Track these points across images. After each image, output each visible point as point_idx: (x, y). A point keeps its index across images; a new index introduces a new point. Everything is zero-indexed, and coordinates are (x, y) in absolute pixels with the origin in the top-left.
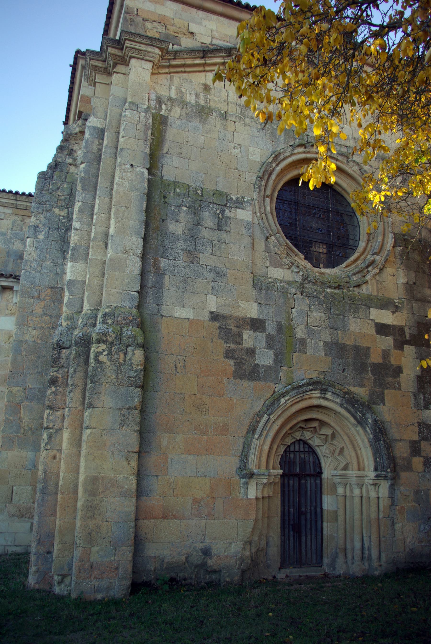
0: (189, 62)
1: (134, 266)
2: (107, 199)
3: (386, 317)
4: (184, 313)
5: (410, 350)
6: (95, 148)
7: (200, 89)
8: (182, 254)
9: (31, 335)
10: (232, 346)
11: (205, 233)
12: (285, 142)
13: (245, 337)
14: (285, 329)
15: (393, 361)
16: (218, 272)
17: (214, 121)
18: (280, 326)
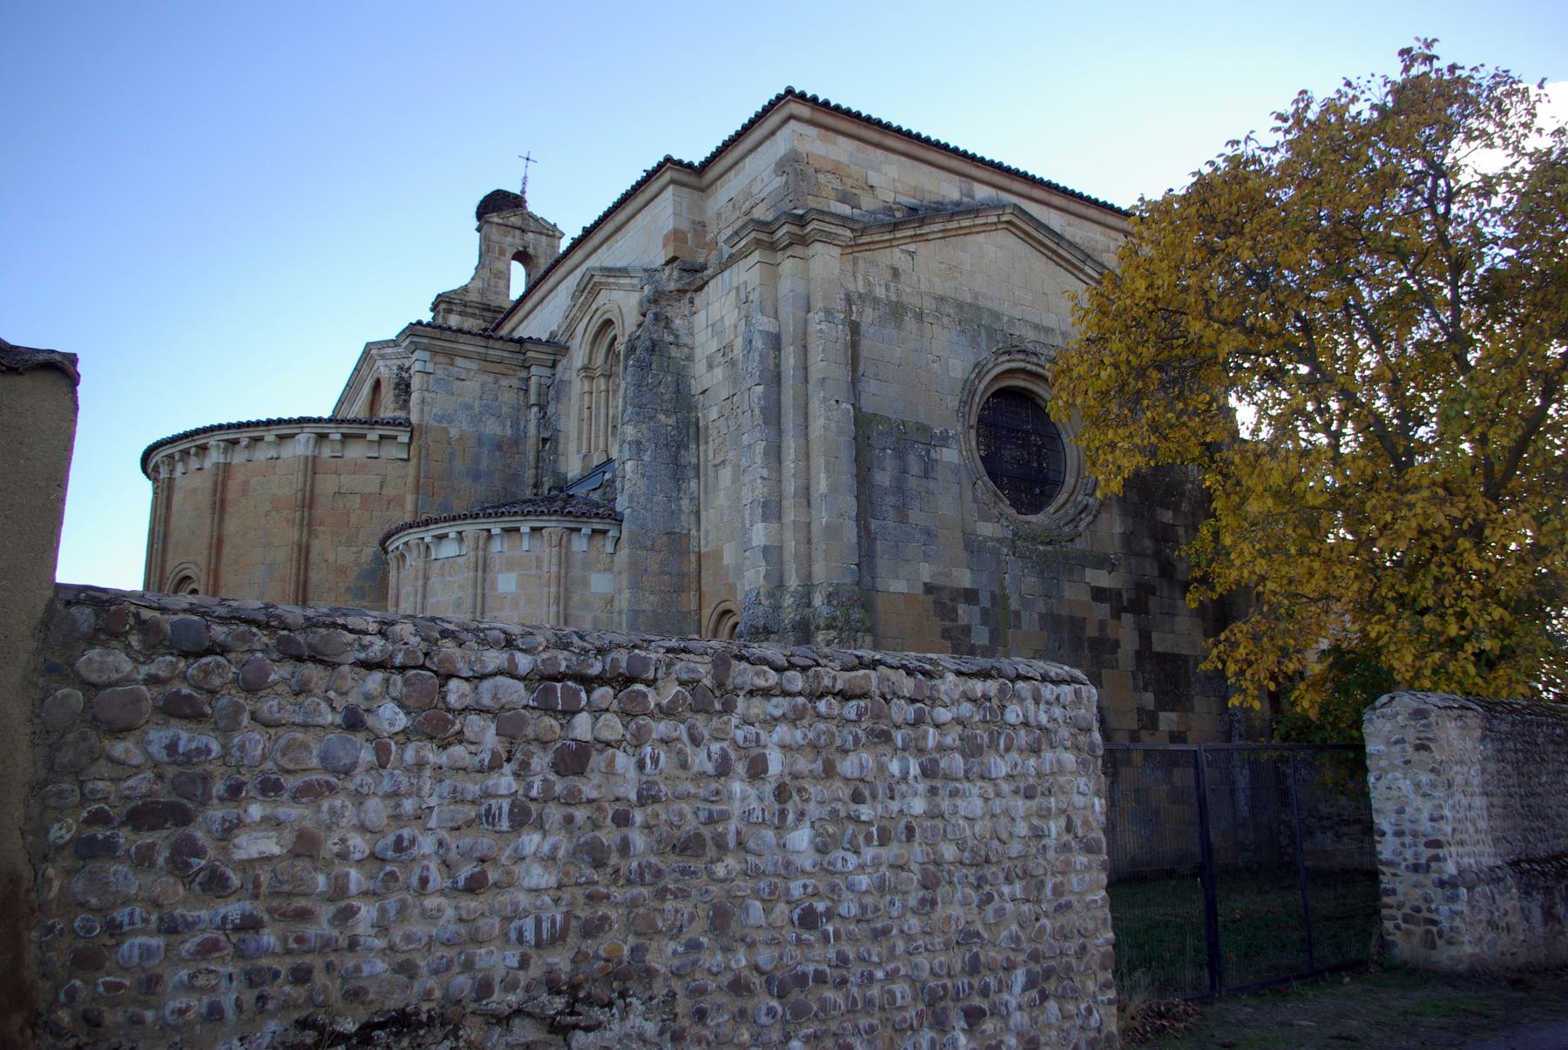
0: (876, 238)
1: (850, 533)
2: (802, 441)
3: (1103, 579)
4: (898, 586)
5: (1127, 618)
6: (771, 361)
7: (888, 275)
8: (891, 511)
9: (649, 602)
10: (948, 624)
11: (912, 483)
12: (989, 349)
13: (960, 612)
14: (999, 600)
15: (1111, 634)
16: (928, 533)
17: (910, 322)
18: (993, 596)
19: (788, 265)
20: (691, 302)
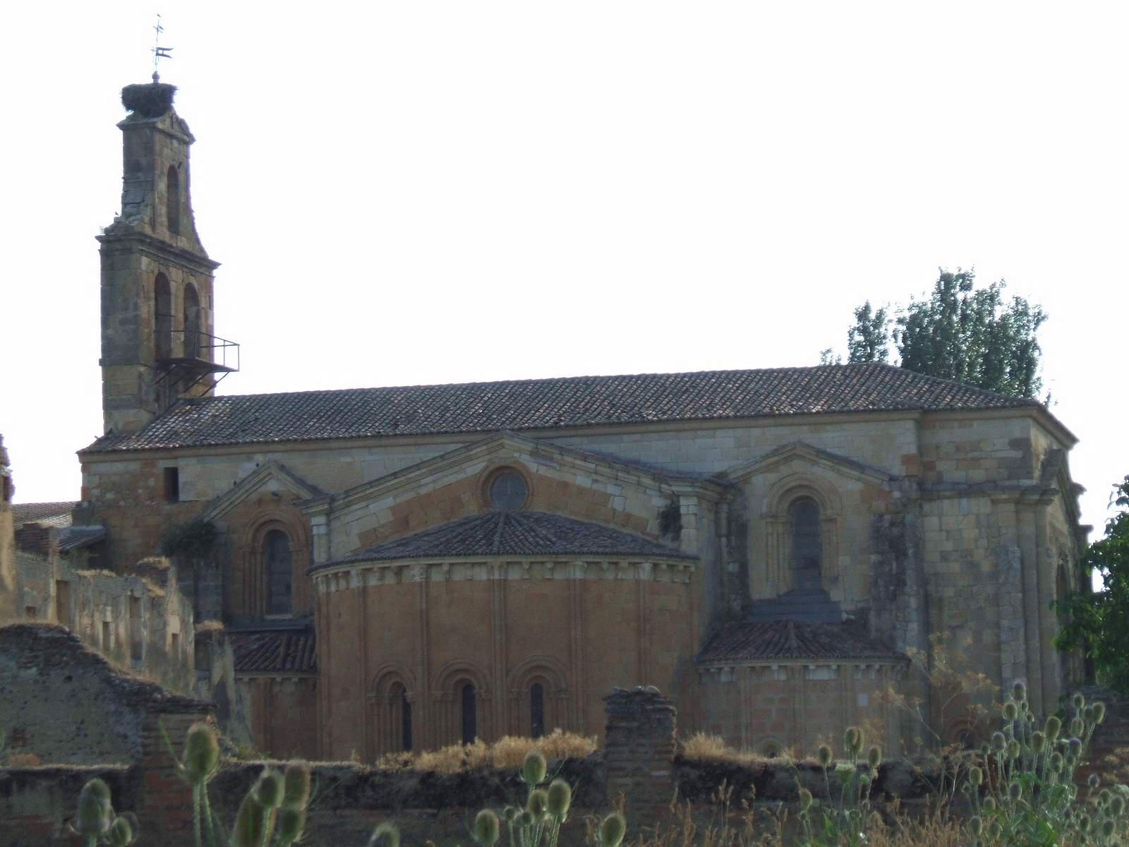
19: (1028, 516)
20: (921, 506)
